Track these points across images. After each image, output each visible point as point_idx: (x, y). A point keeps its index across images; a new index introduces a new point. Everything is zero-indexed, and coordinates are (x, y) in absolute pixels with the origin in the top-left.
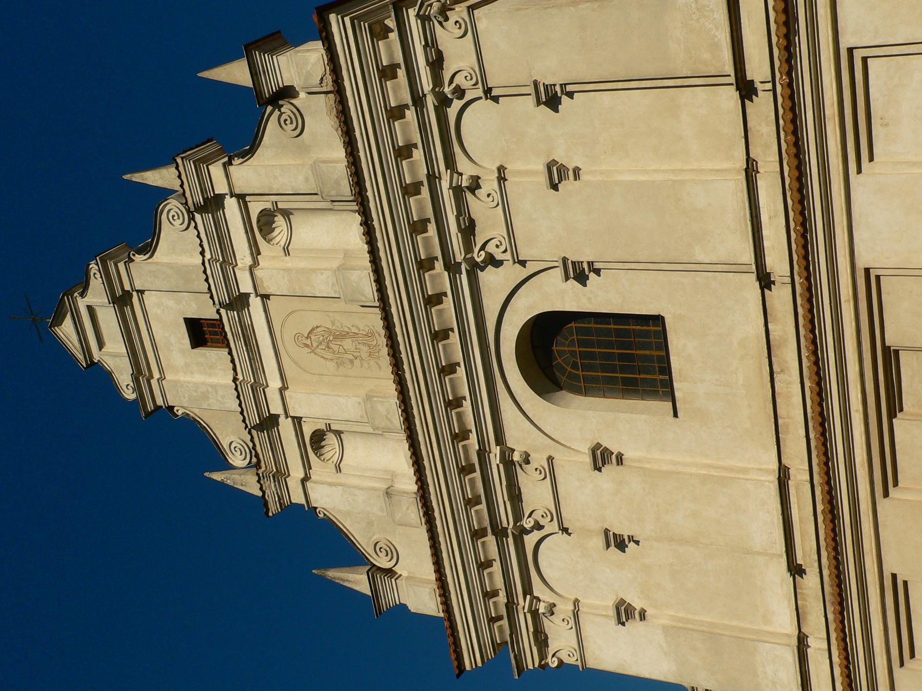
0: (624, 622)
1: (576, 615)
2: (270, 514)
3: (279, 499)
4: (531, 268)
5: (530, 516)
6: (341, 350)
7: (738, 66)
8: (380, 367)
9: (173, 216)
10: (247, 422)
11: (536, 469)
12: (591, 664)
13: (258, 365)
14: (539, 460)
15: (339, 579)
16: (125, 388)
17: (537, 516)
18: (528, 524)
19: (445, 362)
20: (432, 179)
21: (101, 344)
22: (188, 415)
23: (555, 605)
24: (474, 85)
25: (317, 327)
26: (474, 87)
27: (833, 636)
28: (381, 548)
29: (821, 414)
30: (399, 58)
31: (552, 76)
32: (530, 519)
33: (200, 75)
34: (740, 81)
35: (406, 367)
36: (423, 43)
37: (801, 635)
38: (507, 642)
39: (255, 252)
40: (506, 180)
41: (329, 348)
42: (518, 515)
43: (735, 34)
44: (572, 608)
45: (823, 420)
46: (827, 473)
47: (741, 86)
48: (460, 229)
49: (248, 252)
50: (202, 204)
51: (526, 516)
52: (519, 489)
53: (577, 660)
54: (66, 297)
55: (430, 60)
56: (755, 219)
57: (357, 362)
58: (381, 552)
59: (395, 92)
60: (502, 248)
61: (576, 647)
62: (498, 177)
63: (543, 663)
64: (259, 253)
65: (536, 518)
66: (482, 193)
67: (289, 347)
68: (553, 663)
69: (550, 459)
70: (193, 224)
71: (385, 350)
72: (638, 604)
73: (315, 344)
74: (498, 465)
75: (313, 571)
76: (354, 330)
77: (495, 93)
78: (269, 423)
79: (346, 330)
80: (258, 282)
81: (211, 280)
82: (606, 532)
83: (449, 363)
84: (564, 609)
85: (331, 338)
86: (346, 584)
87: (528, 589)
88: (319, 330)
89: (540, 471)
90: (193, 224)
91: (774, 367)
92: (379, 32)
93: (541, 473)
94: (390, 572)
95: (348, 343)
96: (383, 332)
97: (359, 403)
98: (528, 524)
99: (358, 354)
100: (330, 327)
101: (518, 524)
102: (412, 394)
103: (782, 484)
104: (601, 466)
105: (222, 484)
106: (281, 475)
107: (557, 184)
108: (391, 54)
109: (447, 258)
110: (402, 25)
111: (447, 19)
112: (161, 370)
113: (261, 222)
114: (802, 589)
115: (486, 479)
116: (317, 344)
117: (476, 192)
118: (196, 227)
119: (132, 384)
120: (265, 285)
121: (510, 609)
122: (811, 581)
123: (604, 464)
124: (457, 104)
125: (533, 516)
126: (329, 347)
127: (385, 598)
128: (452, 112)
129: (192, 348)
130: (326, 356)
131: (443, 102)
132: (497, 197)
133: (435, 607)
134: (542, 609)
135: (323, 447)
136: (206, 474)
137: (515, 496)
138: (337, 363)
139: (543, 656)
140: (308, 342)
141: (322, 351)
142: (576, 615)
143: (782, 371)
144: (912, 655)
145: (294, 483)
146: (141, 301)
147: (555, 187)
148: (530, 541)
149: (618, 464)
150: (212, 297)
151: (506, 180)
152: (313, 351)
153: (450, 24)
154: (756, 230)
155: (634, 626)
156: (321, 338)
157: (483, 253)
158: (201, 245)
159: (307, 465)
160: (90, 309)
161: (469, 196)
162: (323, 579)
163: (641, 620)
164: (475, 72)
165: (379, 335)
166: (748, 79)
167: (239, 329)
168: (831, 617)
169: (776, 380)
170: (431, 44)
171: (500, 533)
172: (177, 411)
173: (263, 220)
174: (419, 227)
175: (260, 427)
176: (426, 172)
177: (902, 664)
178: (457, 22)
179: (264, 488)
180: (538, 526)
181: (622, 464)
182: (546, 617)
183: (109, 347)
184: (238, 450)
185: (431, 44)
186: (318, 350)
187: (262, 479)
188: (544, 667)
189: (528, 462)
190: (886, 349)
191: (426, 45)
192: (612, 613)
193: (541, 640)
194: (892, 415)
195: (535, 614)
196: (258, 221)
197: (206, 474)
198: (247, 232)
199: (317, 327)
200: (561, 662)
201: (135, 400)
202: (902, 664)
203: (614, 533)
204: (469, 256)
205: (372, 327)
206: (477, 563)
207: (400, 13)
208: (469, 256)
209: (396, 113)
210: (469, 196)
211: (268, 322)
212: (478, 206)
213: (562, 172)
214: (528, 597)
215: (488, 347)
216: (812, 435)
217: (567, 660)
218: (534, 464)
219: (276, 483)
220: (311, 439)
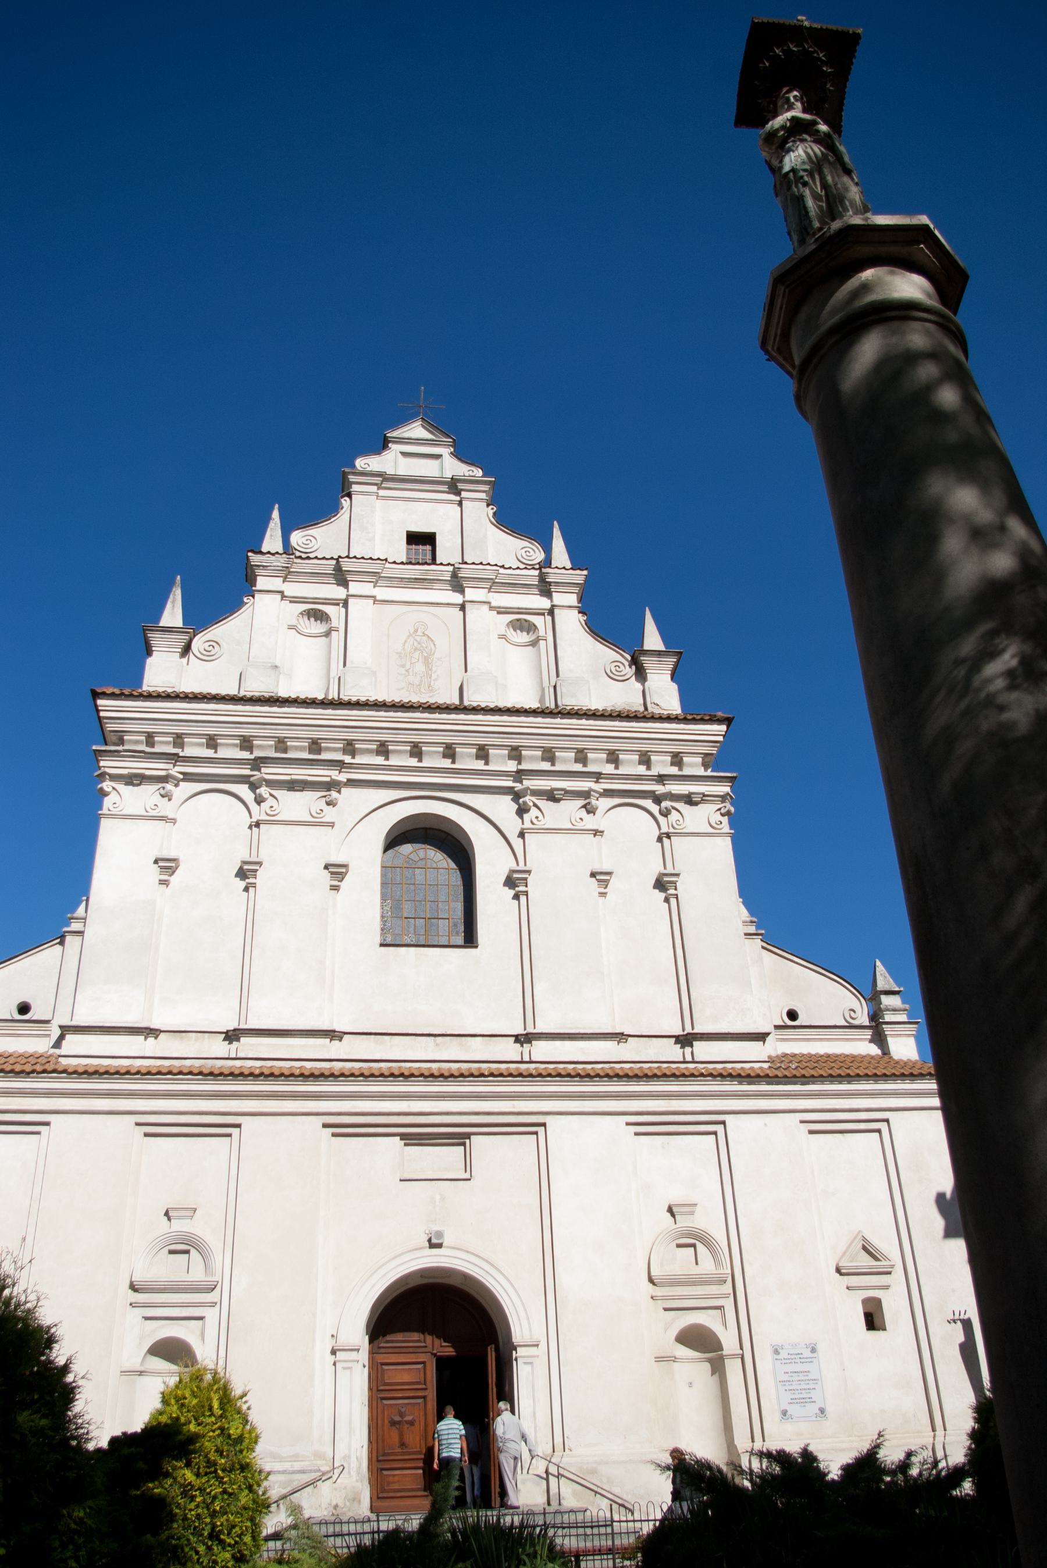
0: (158, 863)
1: (163, 818)
2: (250, 554)
3: (264, 566)
4: (517, 843)
5: (271, 795)
6: (414, 660)
7: (705, 1036)
8: (399, 690)
9: (529, 552)
10: (346, 560)
11: (322, 810)
12: (104, 823)
13: (395, 584)
14: (329, 814)
15: (174, 598)
16: (366, 461)
17: (271, 801)
18: (263, 791)
20: (598, 775)
21: (404, 454)
22: (342, 508)
23: (170, 800)
24: (672, 826)
25: (434, 644)
26: (670, 825)
27: (166, 1063)
28: (213, 647)
29: (412, 1075)
30: (687, 771)
31: (684, 887)
34: (694, 1036)
35: (426, 715)
36: (706, 793)
37: (158, 1033)
39: (502, 611)
40: (594, 836)
42: (271, 784)
43: (730, 1036)
44: (170, 817)
45: (406, 1076)
46: (352, 1075)
48: (553, 790)
49: (502, 604)
50: (547, 580)
51: (274, 792)
53: (109, 810)
54: (451, 440)
55: (693, 796)
56: (581, 1036)
57: (402, 670)
58: (209, 646)
59: (663, 762)
60: (535, 821)
61: (124, 812)
63: (107, 777)
64: (499, 613)
65: (268, 800)
66: (583, 813)
67: (415, 615)
68: (107, 785)
69: (332, 825)
70: (523, 566)
72: (174, 880)
73: (418, 638)
74: (330, 776)
75: (179, 576)
76: (434, 676)
77: (666, 840)
78: (341, 577)
79: (434, 669)
80: (477, 606)
82: (260, 864)
83: (423, 753)
84: (166, 808)
85: (425, 654)
86: (169, 605)
87: (188, 777)
88: (432, 645)
91: (440, 1038)
92: (708, 761)
94: (186, 650)
95: (420, 667)
96: (432, 701)
97: (366, 663)
98: (263, 791)
99: (411, 674)
100: (435, 655)
101: (264, 783)
102: (399, 714)
103: (328, 1033)
104: (330, 870)
105: (269, 518)
106: (287, 574)
107: (595, 877)
108: (691, 765)
109: (528, 773)
110: (720, 780)
111: (722, 815)
112: (385, 498)
113: (524, 622)
114: (209, 1037)
115: (314, 763)
117: (584, 809)
119: (368, 469)
120: (474, 610)
121: (172, 757)
122: (219, 1047)
124: (655, 809)
125: (271, 798)
126: (416, 649)
127: (162, 638)
128: (648, 803)
129: (407, 532)
130: (406, 645)
131: (657, 799)
132: (580, 825)
133: (154, 683)
134: (169, 787)
135: (309, 619)
136: (277, 506)
137: (293, 786)
138: (400, 653)
139: (114, 778)
140: (419, 633)
142: (163, 818)
143: (437, 1045)
144: (146, 1135)
145: (277, 583)
146: (451, 502)
147: (593, 875)
148: (243, 790)
149: (331, 886)
151: (594, 836)
152: (410, 635)
153: (718, 817)
154: (571, 1036)
155: (154, 873)
156: (424, 646)
157: (531, 804)
158: (510, 568)
159: (295, 600)
160: (438, 457)
161: (582, 802)
162: (171, 585)
163: (160, 880)
165: (431, 697)
166: (694, 1043)
167: (432, 577)
168: (188, 1063)
169: (428, 1038)
170: (704, 798)
172: (345, 500)
173: (526, 624)
174: (549, 755)
175: (338, 568)
176: (604, 772)
178: (721, 823)
179: (277, 555)
180: (259, 800)
181: (331, 889)
182: (159, 789)
183: (402, 460)
184: (306, 543)
185: (704, 798)
186: (412, 640)
187: (288, 556)
188: (102, 776)
189: (328, 804)
190: (468, 1136)
191: (704, 795)
192: (166, 854)
193: (134, 780)
194: (403, 1136)
195: (164, 779)
196: (526, 621)
197: (277, 506)
198: (519, 608)
199: (434, 644)
200: (106, 794)
201: (354, 466)
202: (137, 1124)
203: (257, 870)
204: (529, 791)
205: (438, 692)
206: (215, 735)
207: (728, 780)
208: (529, 791)
209: (645, 759)
210: (582, 802)
211: (438, 604)
212: (572, 808)
213: (605, 883)
214: (181, 776)
215: (440, 790)
216: (382, 1065)
217: (108, 802)
218: (326, 808)
219: (281, 568)
220: (320, 610)
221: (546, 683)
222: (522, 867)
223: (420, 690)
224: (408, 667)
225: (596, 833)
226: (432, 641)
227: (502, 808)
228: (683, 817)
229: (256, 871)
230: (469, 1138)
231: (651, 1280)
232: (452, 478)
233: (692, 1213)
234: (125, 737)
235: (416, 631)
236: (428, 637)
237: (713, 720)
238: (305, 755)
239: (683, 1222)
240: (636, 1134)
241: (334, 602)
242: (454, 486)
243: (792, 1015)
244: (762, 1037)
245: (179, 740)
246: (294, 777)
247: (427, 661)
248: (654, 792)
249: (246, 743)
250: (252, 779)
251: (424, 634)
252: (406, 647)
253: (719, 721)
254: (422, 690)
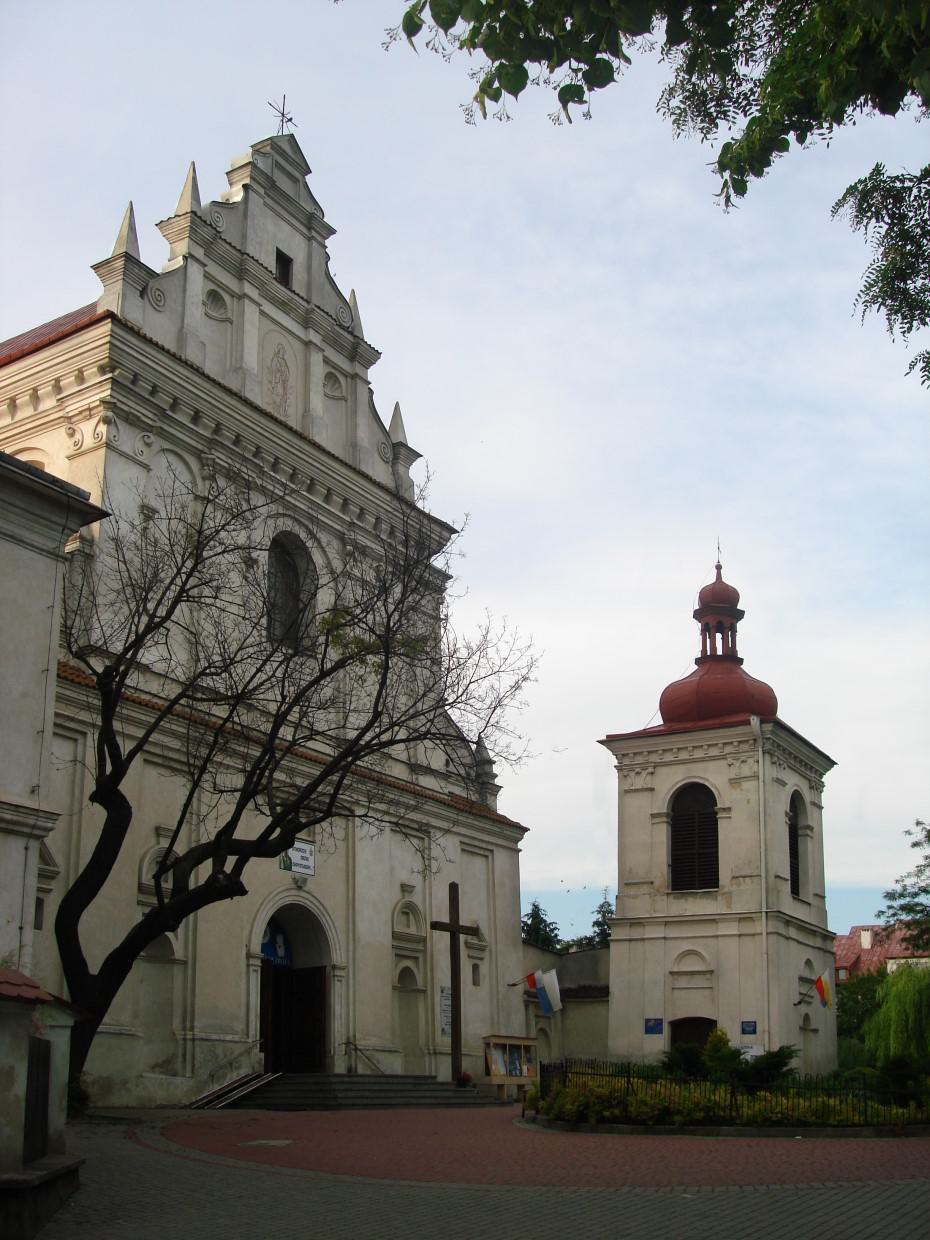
71: (276, 415)
81: (325, 315)
95: (280, 390)
112: (265, 204)
146: (303, 234)
150: (319, 308)
171: (212, 443)
227: (333, 548)
233: (411, 892)
247: (285, 382)
250: (203, 455)
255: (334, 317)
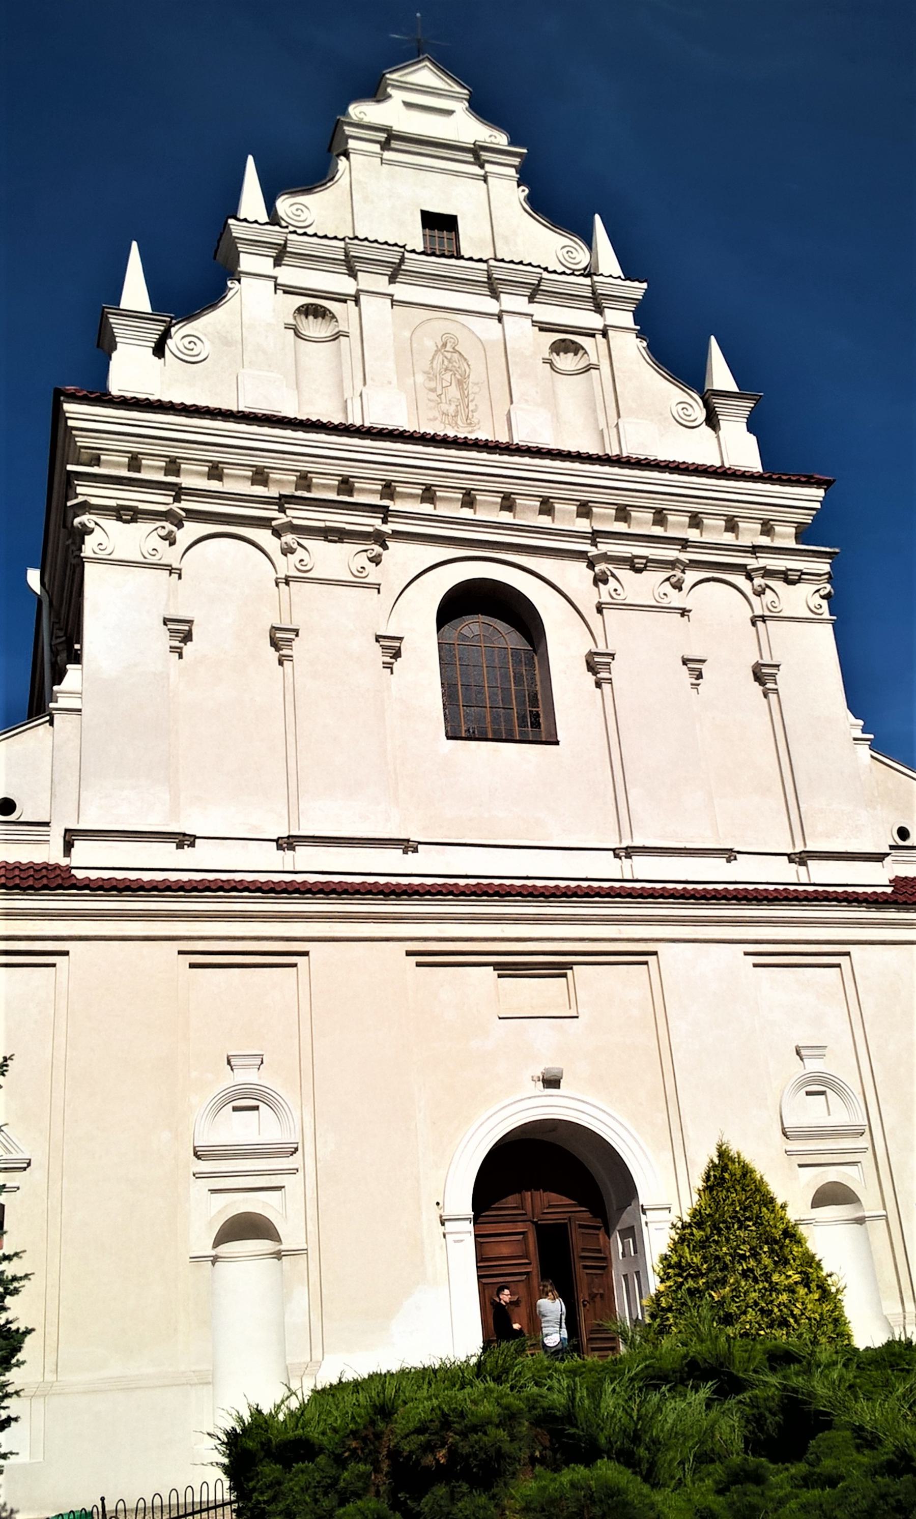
10: (356, 242)
11: (363, 568)
14: (373, 574)
19: (480, 500)
20: (684, 542)
25: (468, 364)
30: (778, 543)
32: (296, 543)
33: (713, 340)
36: (805, 571)
38: (139, 472)
41: (446, 369)
47: (803, 855)
52: (335, 542)
54: (466, 92)
57: (433, 396)
59: (750, 530)
60: (613, 594)
62: (685, 609)
64: (541, 329)
67: (441, 324)
71: (451, 434)
72: (188, 649)
73: (449, 355)
76: (471, 407)
77: (760, 624)
89: (361, 572)
90: (568, 272)
93: (359, 571)
96: (472, 436)
100: (471, 380)
109: (603, 535)
111: (822, 597)
112: (391, 162)
116: (449, 357)
118: (564, 273)
123: (383, 647)
126: (446, 369)
130: (435, 362)
132: (665, 602)
135: (307, 317)
140: (448, 348)
141: (440, 360)
144: (192, 966)
146: (473, 177)
153: (817, 600)
156: (457, 366)
160: (450, 112)
163: (171, 647)
164: (779, 612)
166: (809, 862)
176: (690, 539)
177: (181, 953)
178: (821, 607)
182: (156, 529)
184: (299, 212)
186: (441, 356)
190: (569, 966)
194: (497, 966)
199: (468, 364)
201: (348, 116)
205: (477, 426)
207: (828, 556)
214: (183, 514)
220: (322, 307)
221: (602, 425)
222: (602, 648)
223: (456, 423)
224: (439, 392)
225: (684, 612)
226: (465, 360)
228: (778, 597)
229: (291, 640)
230: (571, 969)
231: (785, 1134)
232: (474, 144)
234: (103, 457)
235: (445, 345)
236: (460, 354)
237: (809, 482)
238: (333, 496)
239: (813, 1065)
240: (755, 965)
241: (341, 299)
242: (477, 153)
243: (903, 833)
244: (879, 857)
245: (173, 467)
246: (329, 524)
248: (745, 566)
249: (260, 476)
250: (274, 523)
251: (456, 351)
252: (434, 366)
253: (818, 484)
254: (459, 422)
255: (560, 269)
